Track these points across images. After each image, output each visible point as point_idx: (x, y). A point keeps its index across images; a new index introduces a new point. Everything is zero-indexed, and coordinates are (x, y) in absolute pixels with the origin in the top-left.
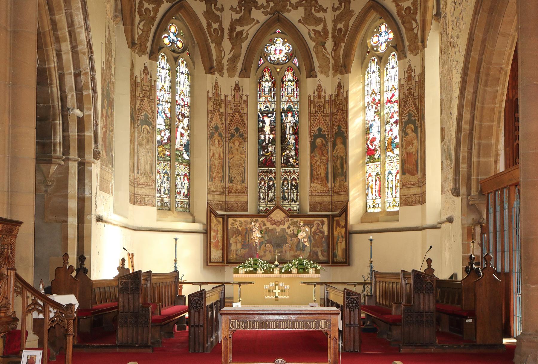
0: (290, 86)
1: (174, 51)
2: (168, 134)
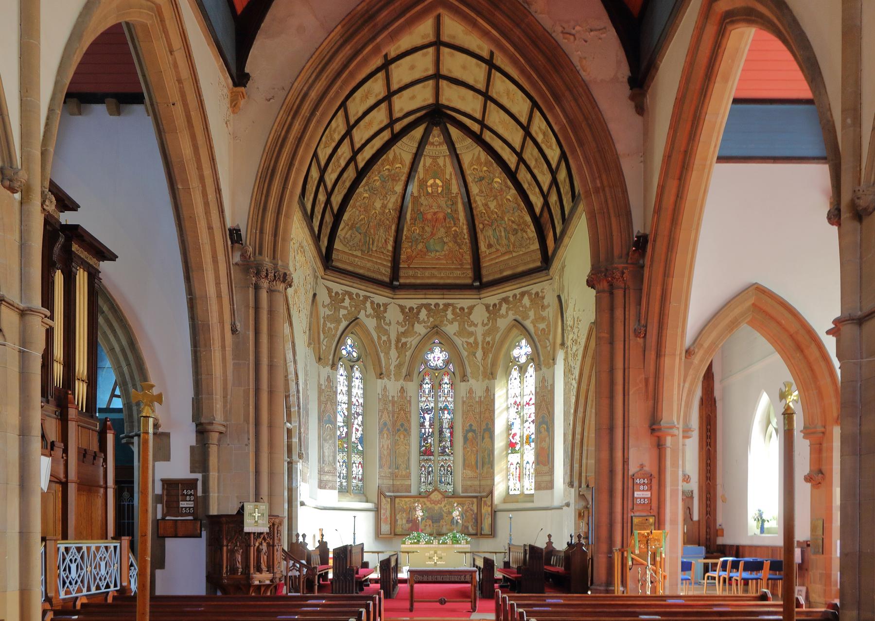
0: (446, 387)
1: (350, 360)
2: (346, 430)
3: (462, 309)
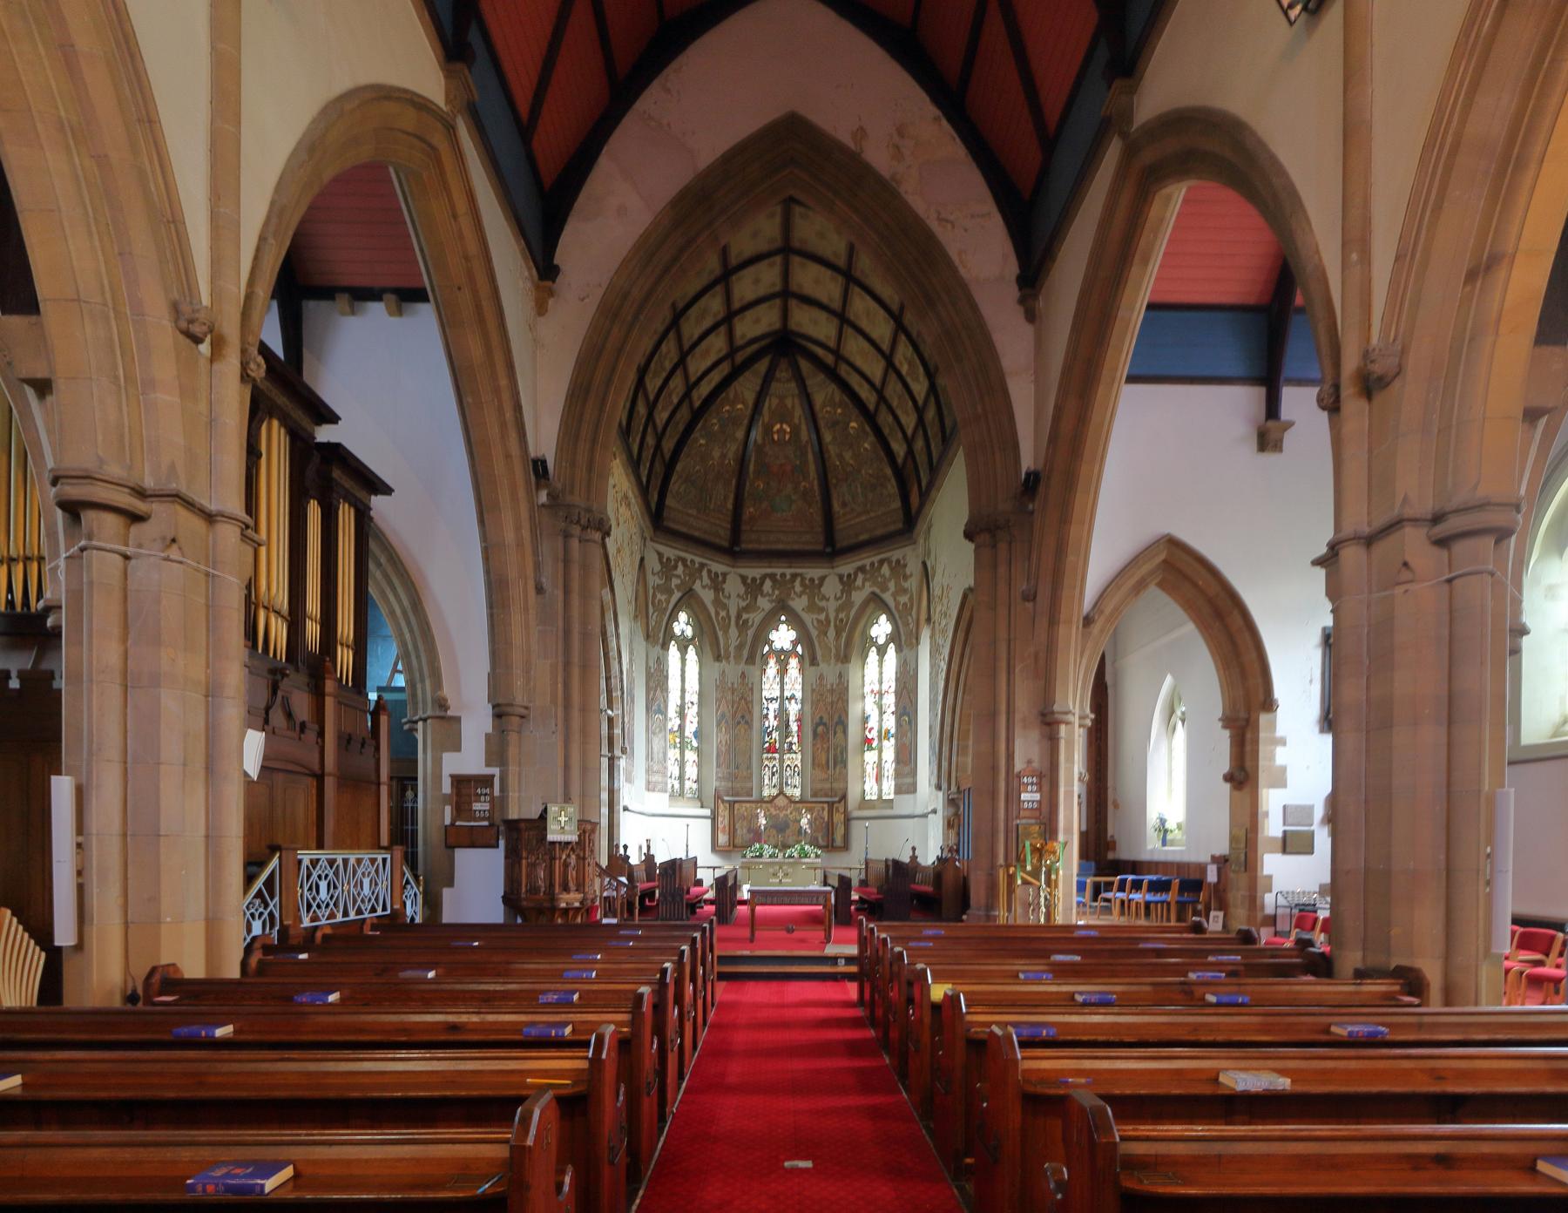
3: (812, 580)
